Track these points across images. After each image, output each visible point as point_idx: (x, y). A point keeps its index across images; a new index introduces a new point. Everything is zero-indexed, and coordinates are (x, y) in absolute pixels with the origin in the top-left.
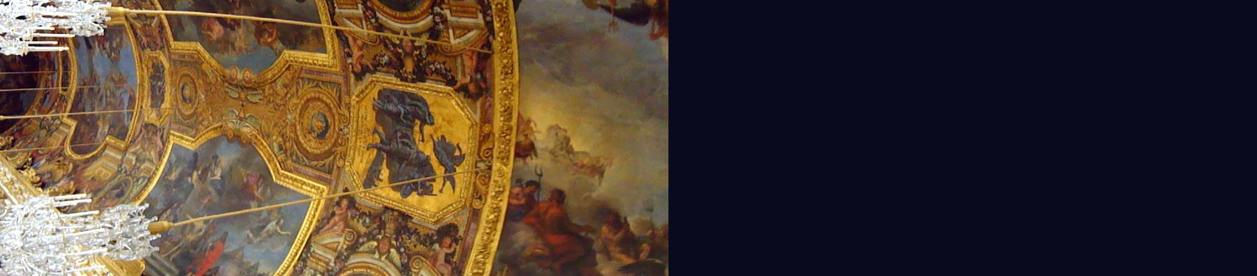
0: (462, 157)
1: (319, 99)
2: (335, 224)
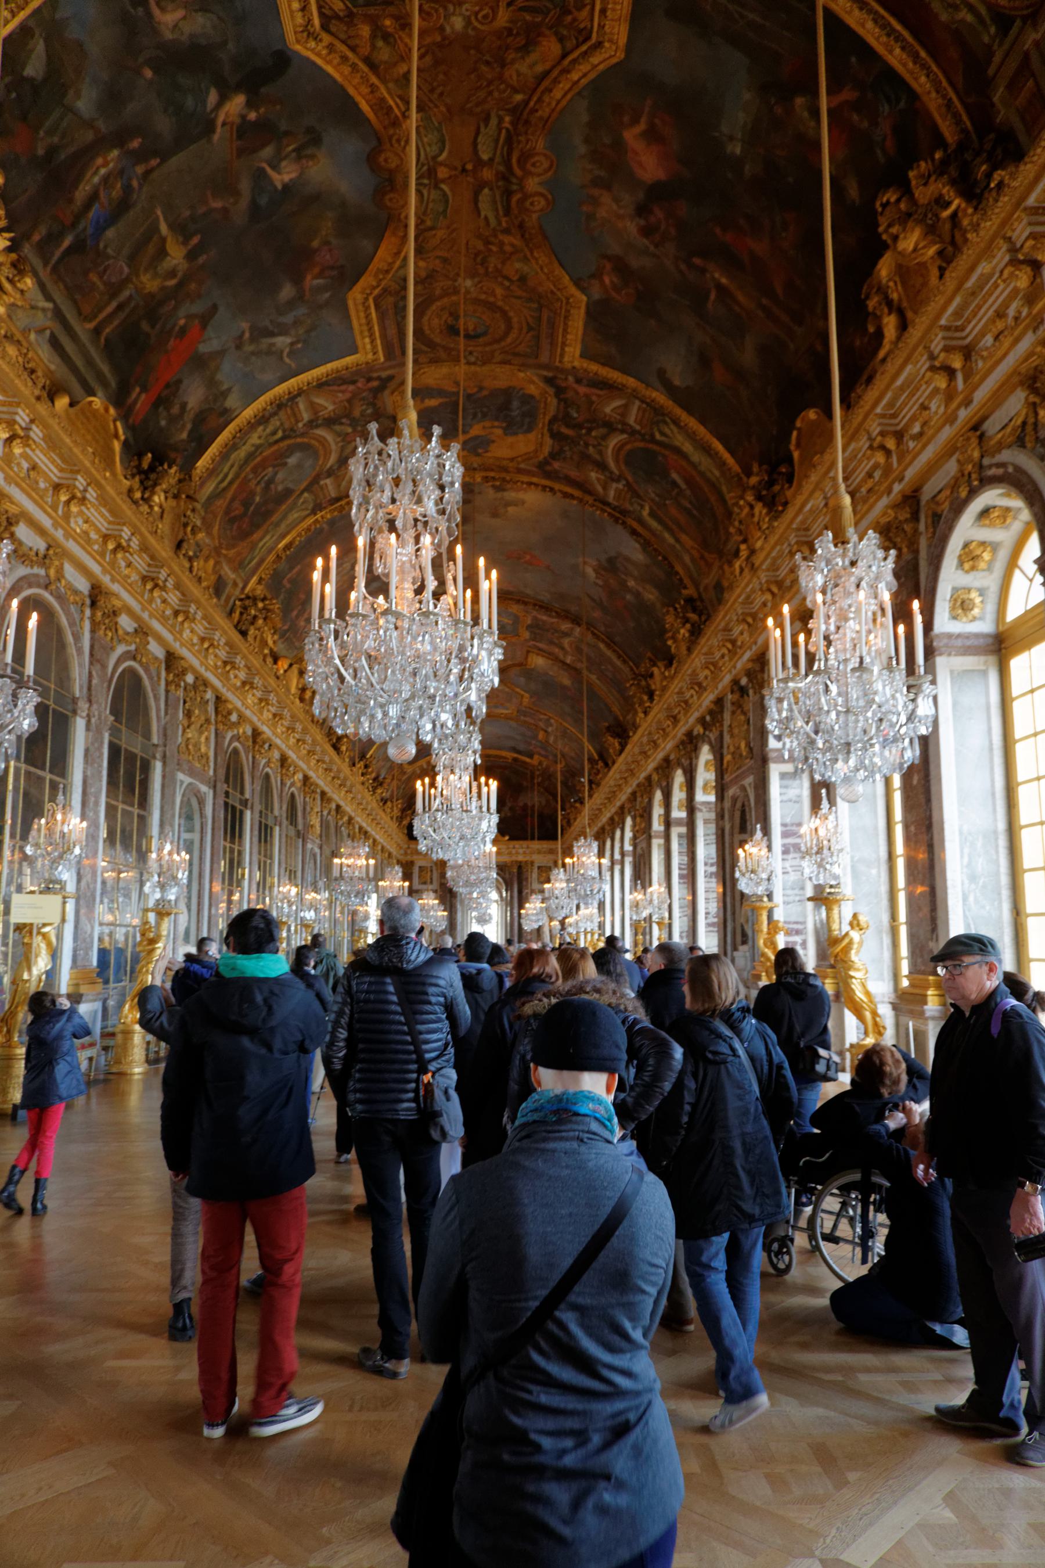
0: (478, 455)
2: (343, 392)
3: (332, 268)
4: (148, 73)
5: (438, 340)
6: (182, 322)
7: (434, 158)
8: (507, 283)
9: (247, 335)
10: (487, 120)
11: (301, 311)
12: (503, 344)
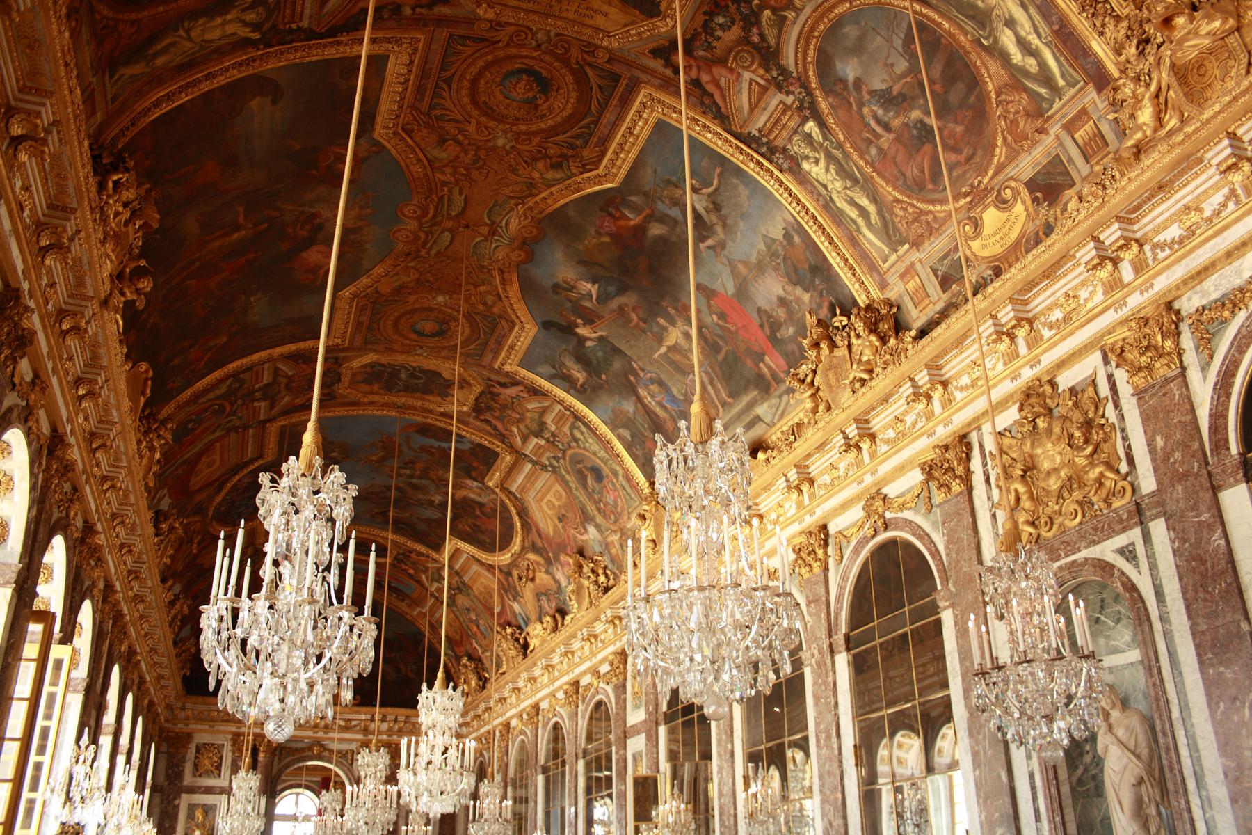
1: (474, 82)
3: (610, 214)
4: (604, 377)
5: (569, 78)
6: (715, 317)
7: (486, 240)
8: (460, 137)
9: (710, 242)
10: (439, 252)
11: (661, 207)
12: (490, 58)
